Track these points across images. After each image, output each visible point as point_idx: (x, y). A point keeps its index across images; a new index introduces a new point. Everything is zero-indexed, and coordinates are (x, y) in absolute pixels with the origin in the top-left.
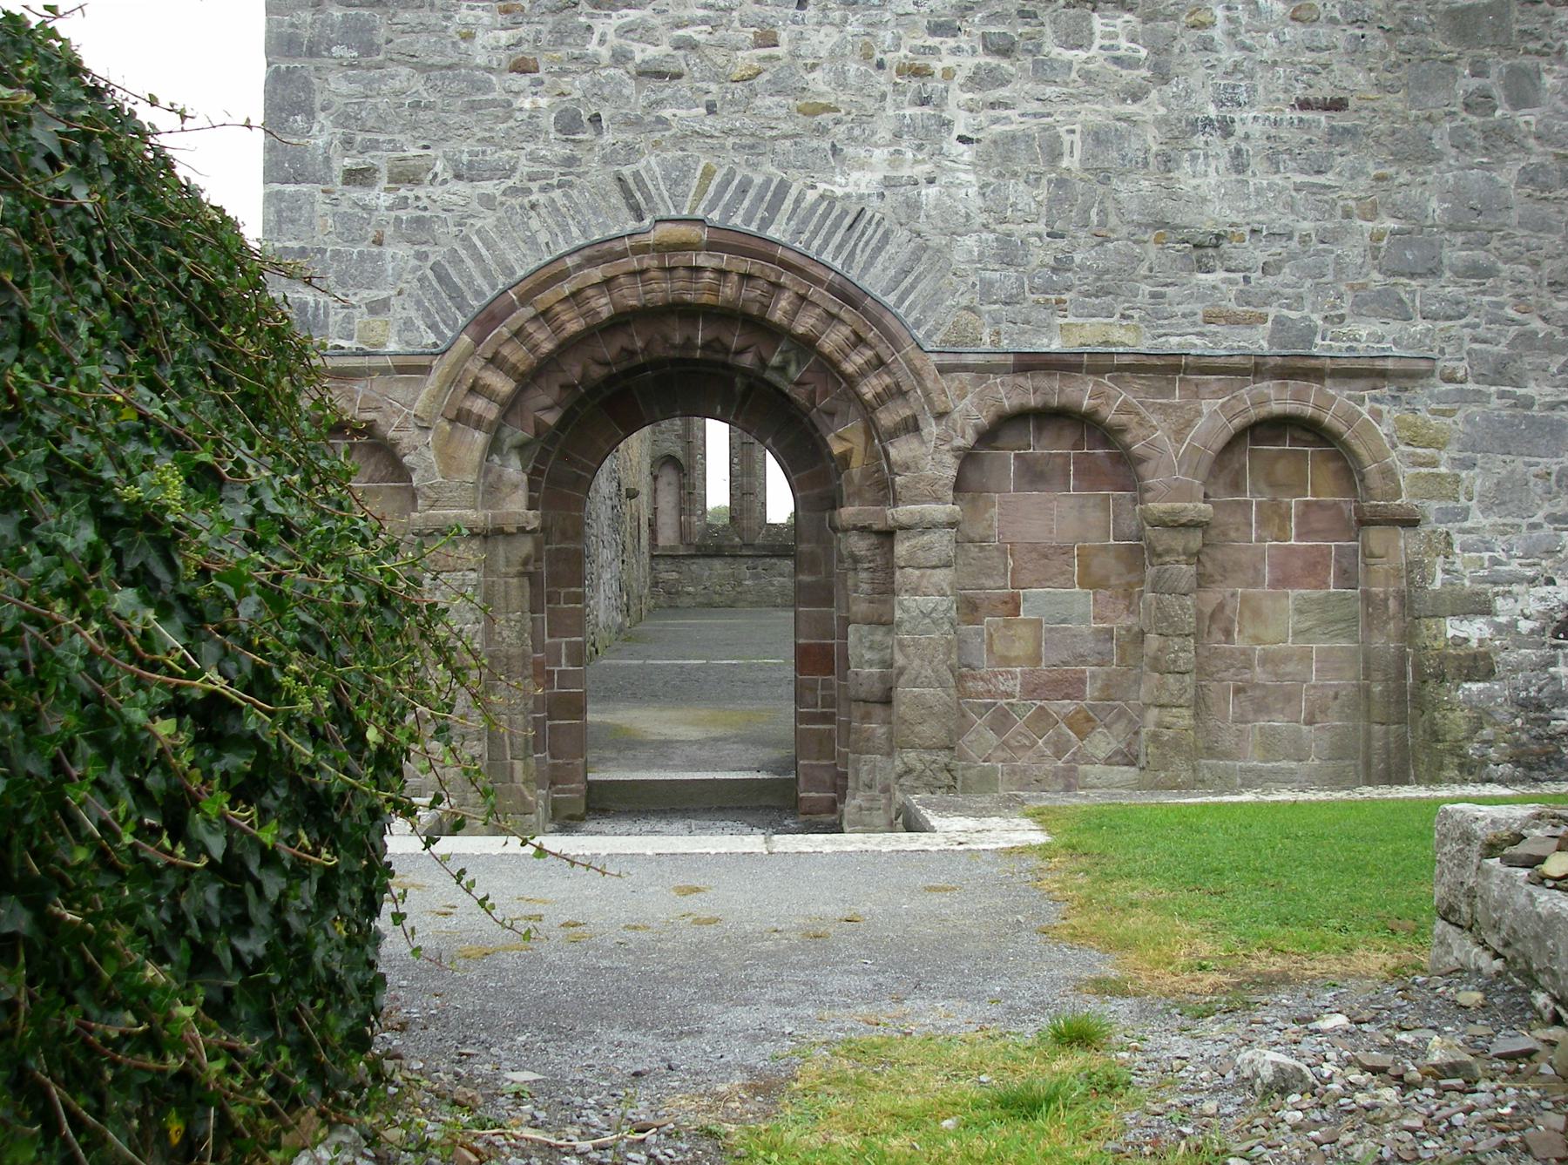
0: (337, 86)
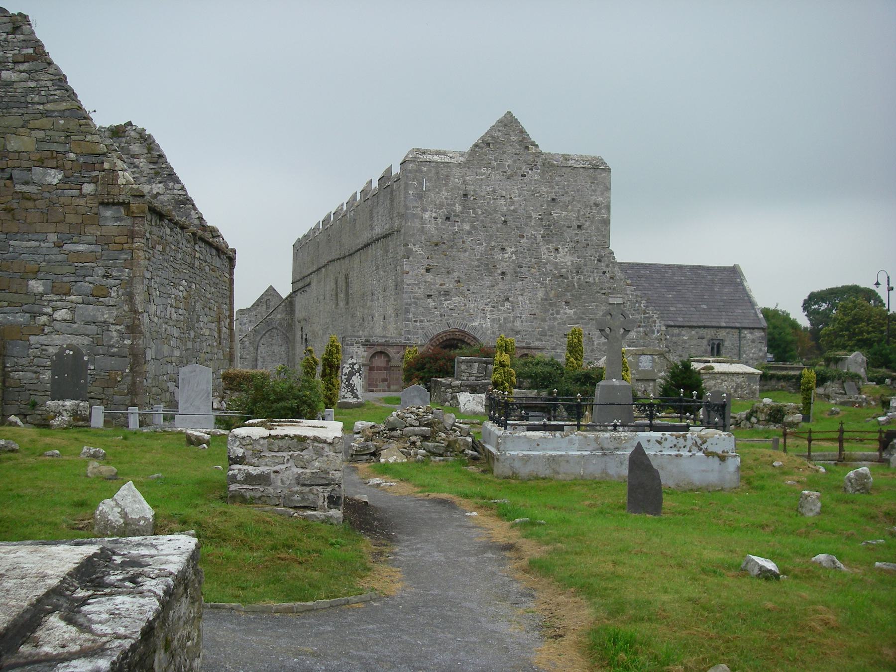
0: (413, 310)
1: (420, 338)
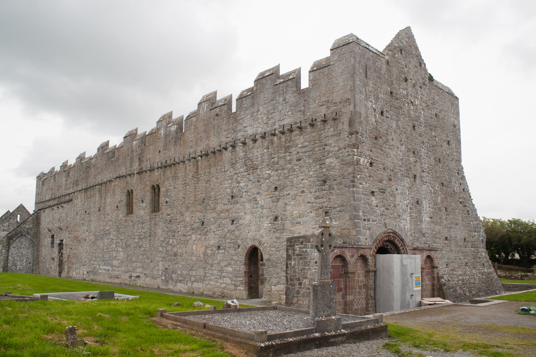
1: (368, 240)
